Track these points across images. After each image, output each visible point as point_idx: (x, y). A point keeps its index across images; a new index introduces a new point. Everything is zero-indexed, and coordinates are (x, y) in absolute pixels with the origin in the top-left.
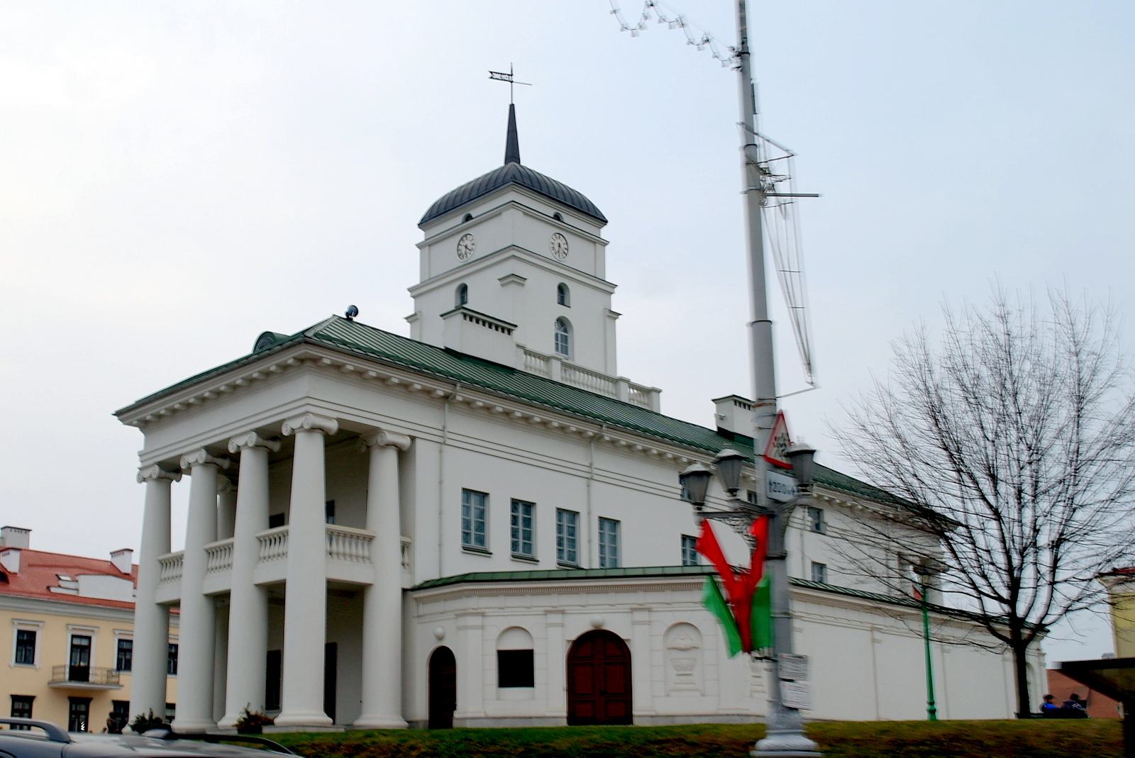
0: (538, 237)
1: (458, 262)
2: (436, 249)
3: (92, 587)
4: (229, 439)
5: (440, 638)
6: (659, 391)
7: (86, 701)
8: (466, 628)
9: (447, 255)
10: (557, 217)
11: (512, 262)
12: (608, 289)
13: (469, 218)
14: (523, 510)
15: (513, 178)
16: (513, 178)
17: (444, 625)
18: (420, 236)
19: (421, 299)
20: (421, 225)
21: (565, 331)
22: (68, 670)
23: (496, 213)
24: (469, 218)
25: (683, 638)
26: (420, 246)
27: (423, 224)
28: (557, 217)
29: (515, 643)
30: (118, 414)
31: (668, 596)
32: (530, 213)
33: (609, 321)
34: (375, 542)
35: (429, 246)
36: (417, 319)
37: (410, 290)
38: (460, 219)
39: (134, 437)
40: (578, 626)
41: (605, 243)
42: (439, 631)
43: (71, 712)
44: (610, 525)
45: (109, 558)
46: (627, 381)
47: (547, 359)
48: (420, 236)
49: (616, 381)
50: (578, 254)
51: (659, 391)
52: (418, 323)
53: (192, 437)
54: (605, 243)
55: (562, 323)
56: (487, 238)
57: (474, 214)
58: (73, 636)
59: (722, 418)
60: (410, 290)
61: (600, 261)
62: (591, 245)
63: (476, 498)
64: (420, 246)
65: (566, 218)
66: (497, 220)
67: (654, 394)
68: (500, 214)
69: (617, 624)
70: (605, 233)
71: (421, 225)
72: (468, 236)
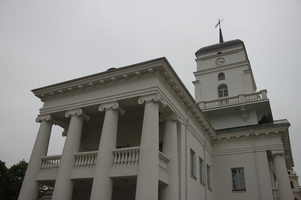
9: (211, 63)
13: (220, 53)
24: (220, 53)
35: (202, 60)
36: (199, 83)
37: (194, 73)
38: (216, 53)
57: (223, 52)
60: (194, 73)
68: (238, 52)
71: (197, 54)
72: (221, 59)
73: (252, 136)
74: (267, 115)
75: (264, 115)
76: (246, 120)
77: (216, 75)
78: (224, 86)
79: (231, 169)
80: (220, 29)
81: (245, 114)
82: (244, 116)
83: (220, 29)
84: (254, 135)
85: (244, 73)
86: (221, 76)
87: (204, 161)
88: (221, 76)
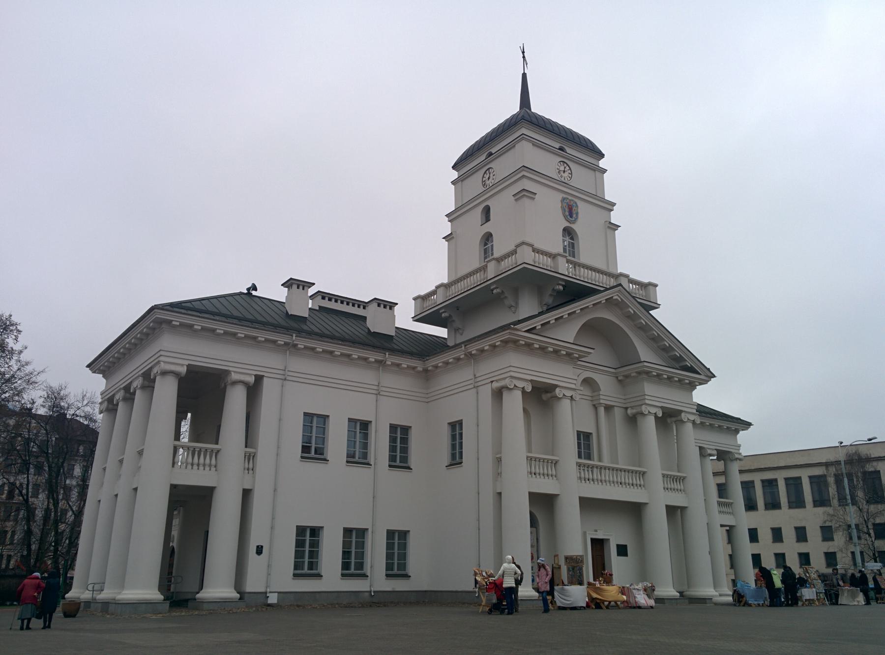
0: (546, 163)
6: (656, 286)
9: (475, 185)
11: (525, 180)
12: (609, 206)
15: (526, 121)
16: (526, 121)
18: (455, 175)
19: (454, 222)
20: (454, 167)
21: (572, 238)
23: (510, 147)
24: (491, 154)
26: (453, 183)
28: (561, 149)
32: (537, 145)
33: (609, 231)
41: (604, 171)
46: (627, 276)
47: (554, 256)
48: (455, 175)
50: (580, 178)
51: (656, 286)
52: (453, 240)
54: (604, 171)
55: (568, 232)
56: (502, 167)
57: (493, 151)
62: (592, 172)
64: (453, 183)
65: (569, 150)
66: (512, 151)
67: (651, 287)
70: (602, 163)
71: (454, 167)
73: (470, 356)
74: (561, 288)
75: (553, 289)
76: (513, 309)
78: (488, 238)
79: (449, 424)
80: (524, 76)
81: (506, 297)
82: (510, 301)
83: (524, 76)
84: (470, 353)
85: (516, 200)
87: (373, 424)
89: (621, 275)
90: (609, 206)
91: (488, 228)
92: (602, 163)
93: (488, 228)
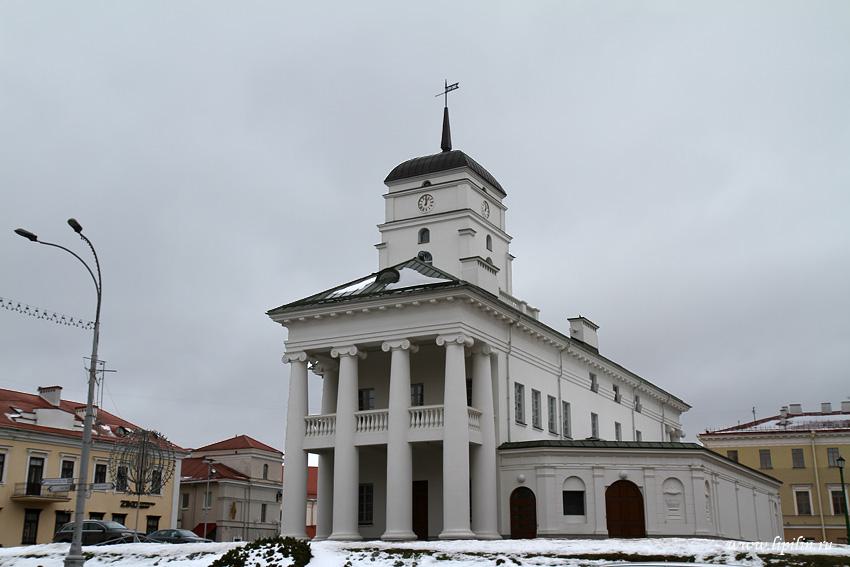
1: (419, 213)
2: (400, 201)
3: (47, 418)
4: (383, 341)
5: (521, 481)
7: (38, 512)
8: (544, 476)
9: (409, 207)
10: (484, 189)
11: (469, 220)
12: (507, 239)
13: (427, 184)
14: (536, 394)
16: (450, 161)
17: (524, 473)
19: (386, 234)
22: (26, 487)
24: (427, 184)
25: (673, 488)
27: (389, 180)
28: (484, 189)
29: (574, 487)
30: (270, 313)
31: (664, 461)
32: (474, 188)
34: (483, 416)
39: (282, 332)
40: (611, 478)
41: (505, 209)
42: (522, 476)
43: (26, 521)
44: (566, 405)
45: (37, 393)
46: (525, 304)
48: (386, 190)
49: (520, 303)
52: (386, 250)
53: (344, 338)
54: (505, 209)
56: (442, 200)
57: (432, 181)
58: (32, 458)
59: (575, 332)
61: (502, 218)
62: (497, 210)
63: (519, 387)
65: (488, 191)
69: (635, 478)
70: (504, 202)
77: (415, 233)
80: (446, 109)
83: (446, 109)
86: (424, 236)
88: (424, 236)
89: (523, 303)
90: (507, 239)
91: (425, 248)
92: (504, 202)
93: (425, 248)
